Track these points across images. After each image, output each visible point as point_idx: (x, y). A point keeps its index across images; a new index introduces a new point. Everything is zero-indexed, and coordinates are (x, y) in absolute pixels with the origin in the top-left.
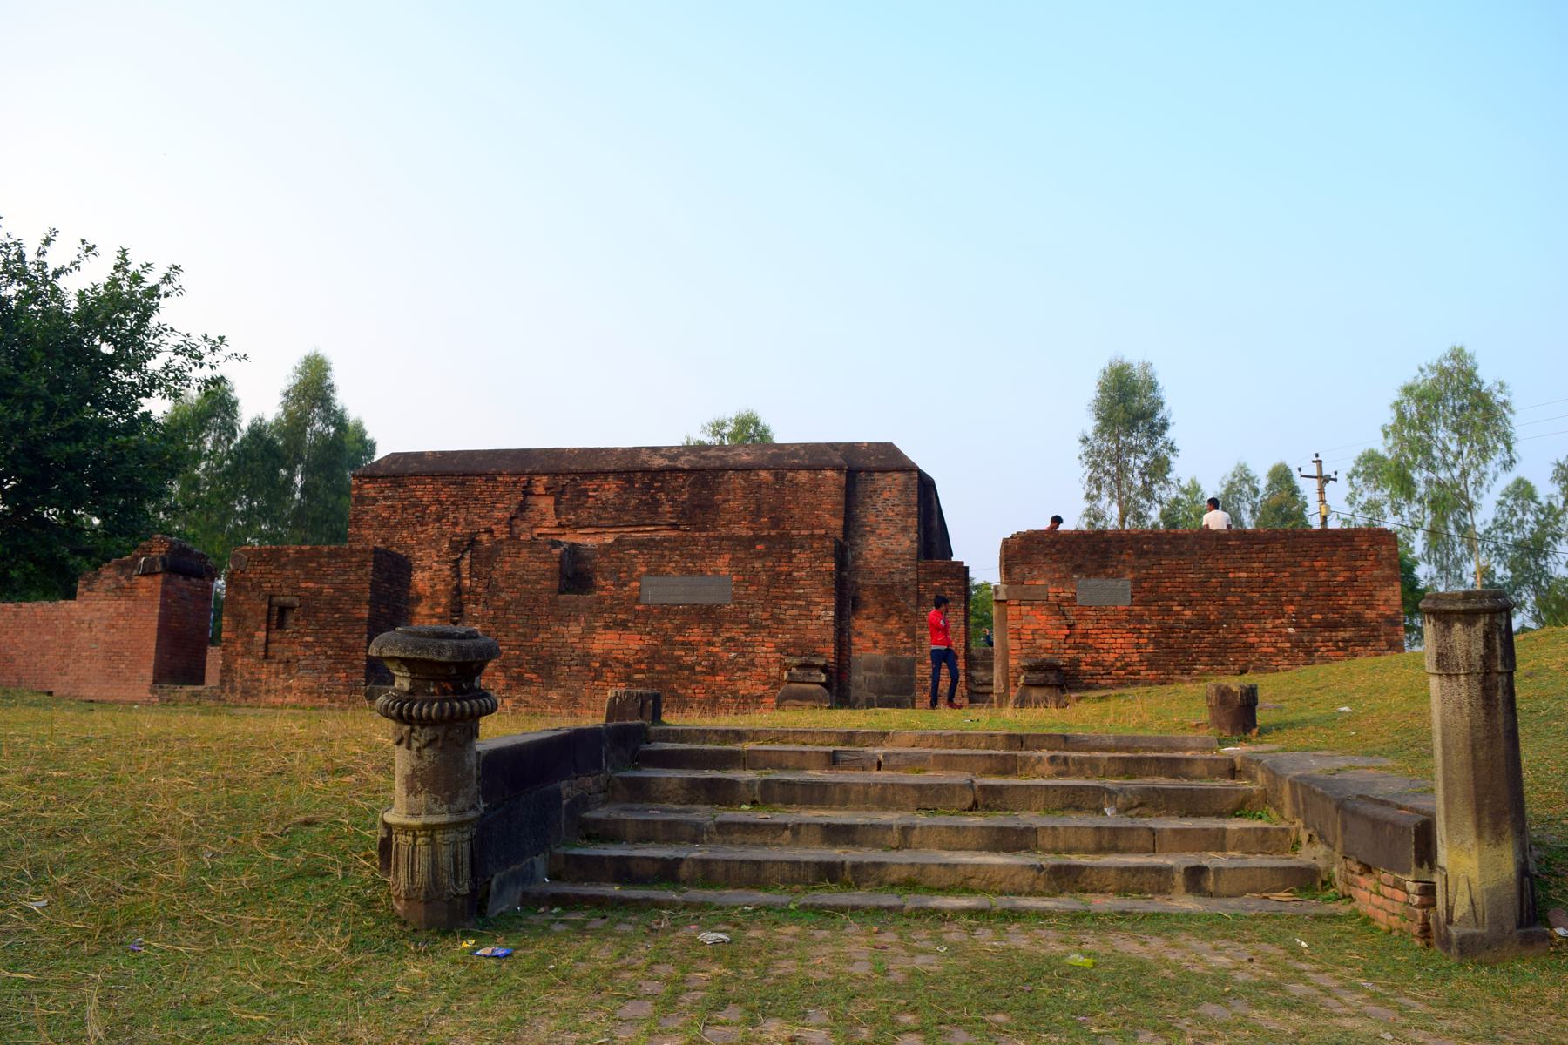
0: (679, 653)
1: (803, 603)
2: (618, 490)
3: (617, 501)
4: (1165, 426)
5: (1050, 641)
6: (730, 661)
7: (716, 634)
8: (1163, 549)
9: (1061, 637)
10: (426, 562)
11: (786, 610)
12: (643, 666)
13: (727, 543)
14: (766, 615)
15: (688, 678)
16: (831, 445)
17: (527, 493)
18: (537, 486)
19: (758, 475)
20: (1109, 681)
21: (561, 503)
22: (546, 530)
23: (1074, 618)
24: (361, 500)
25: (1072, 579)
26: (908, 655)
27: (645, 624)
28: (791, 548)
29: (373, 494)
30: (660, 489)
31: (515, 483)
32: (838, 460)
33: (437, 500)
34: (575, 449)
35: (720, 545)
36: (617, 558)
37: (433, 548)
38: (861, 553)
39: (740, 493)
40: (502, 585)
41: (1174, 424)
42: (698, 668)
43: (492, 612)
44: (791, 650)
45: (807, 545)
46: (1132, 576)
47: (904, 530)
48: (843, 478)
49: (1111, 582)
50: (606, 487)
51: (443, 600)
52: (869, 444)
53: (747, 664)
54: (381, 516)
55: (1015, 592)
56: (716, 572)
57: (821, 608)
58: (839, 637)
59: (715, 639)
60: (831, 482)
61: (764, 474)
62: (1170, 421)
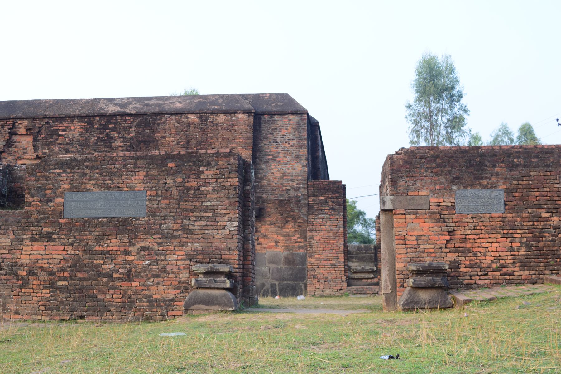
0: (98, 262)
1: (210, 215)
2: (82, 130)
3: (80, 138)
4: (460, 96)
5: (432, 246)
6: (144, 269)
7: (131, 244)
8: (531, 162)
9: (442, 242)
11: (195, 221)
12: (66, 274)
13: (142, 161)
14: (177, 226)
15: (107, 285)
16: (240, 95)
17: (12, 133)
18: (19, 128)
19: (187, 118)
20: (486, 281)
21: (38, 141)
22: (27, 162)
23: (454, 224)
25: (451, 191)
26: (301, 252)
27: (68, 236)
28: (200, 166)
30: (114, 129)
31: (3, 126)
32: (247, 106)
34: (50, 100)
35: (135, 164)
36: (43, 176)
38: (265, 176)
39: (174, 131)
41: (465, 94)
42: (115, 275)
44: (200, 257)
45: (213, 163)
46: (505, 187)
47: (298, 157)
48: (251, 120)
49: (485, 192)
50: (73, 128)
52: (271, 95)
53: (160, 271)
55: (401, 202)
56: (132, 188)
57: (226, 219)
58: (243, 245)
59: (131, 248)
60: (242, 122)
61: (192, 117)
62: (464, 93)
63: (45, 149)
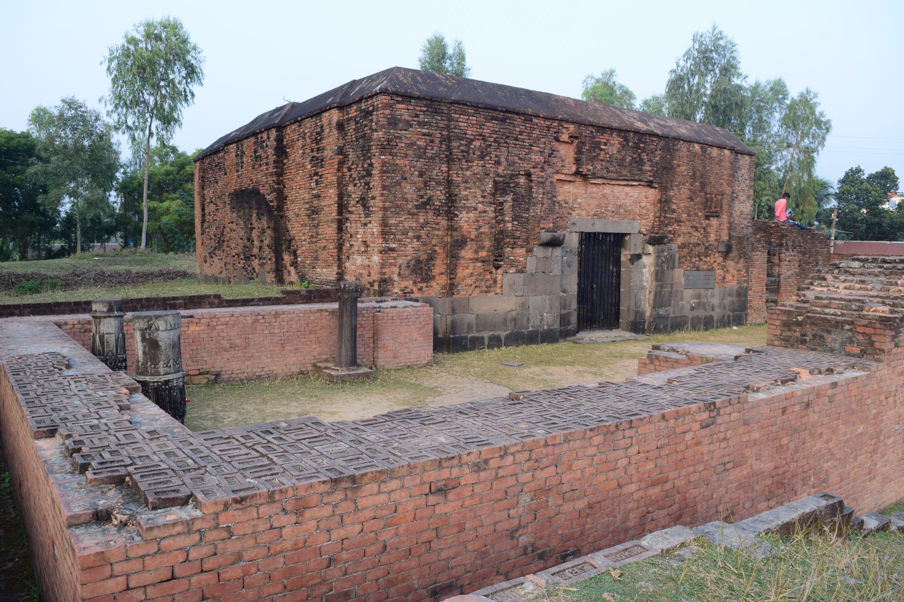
10: (471, 203)
18: (563, 133)
22: (563, 177)
24: (393, 122)
29: (407, 118)
30: (644, 150)
31: (548, 128)
33: (481, 135)
37: (478, 188)
50: (612, 142)
51: (487, 244)
54: (415, 144)
60: (727, 159)
63: (589, 164)
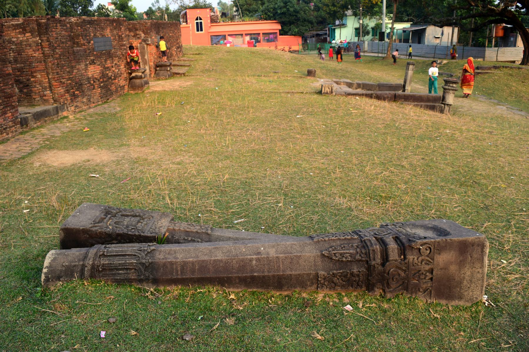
40: (56, 45)
43: (56, 61)
